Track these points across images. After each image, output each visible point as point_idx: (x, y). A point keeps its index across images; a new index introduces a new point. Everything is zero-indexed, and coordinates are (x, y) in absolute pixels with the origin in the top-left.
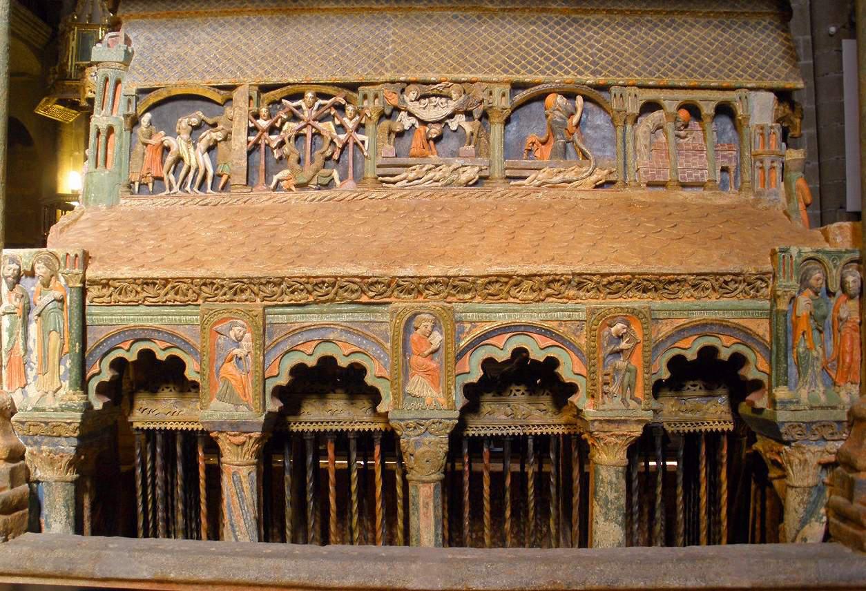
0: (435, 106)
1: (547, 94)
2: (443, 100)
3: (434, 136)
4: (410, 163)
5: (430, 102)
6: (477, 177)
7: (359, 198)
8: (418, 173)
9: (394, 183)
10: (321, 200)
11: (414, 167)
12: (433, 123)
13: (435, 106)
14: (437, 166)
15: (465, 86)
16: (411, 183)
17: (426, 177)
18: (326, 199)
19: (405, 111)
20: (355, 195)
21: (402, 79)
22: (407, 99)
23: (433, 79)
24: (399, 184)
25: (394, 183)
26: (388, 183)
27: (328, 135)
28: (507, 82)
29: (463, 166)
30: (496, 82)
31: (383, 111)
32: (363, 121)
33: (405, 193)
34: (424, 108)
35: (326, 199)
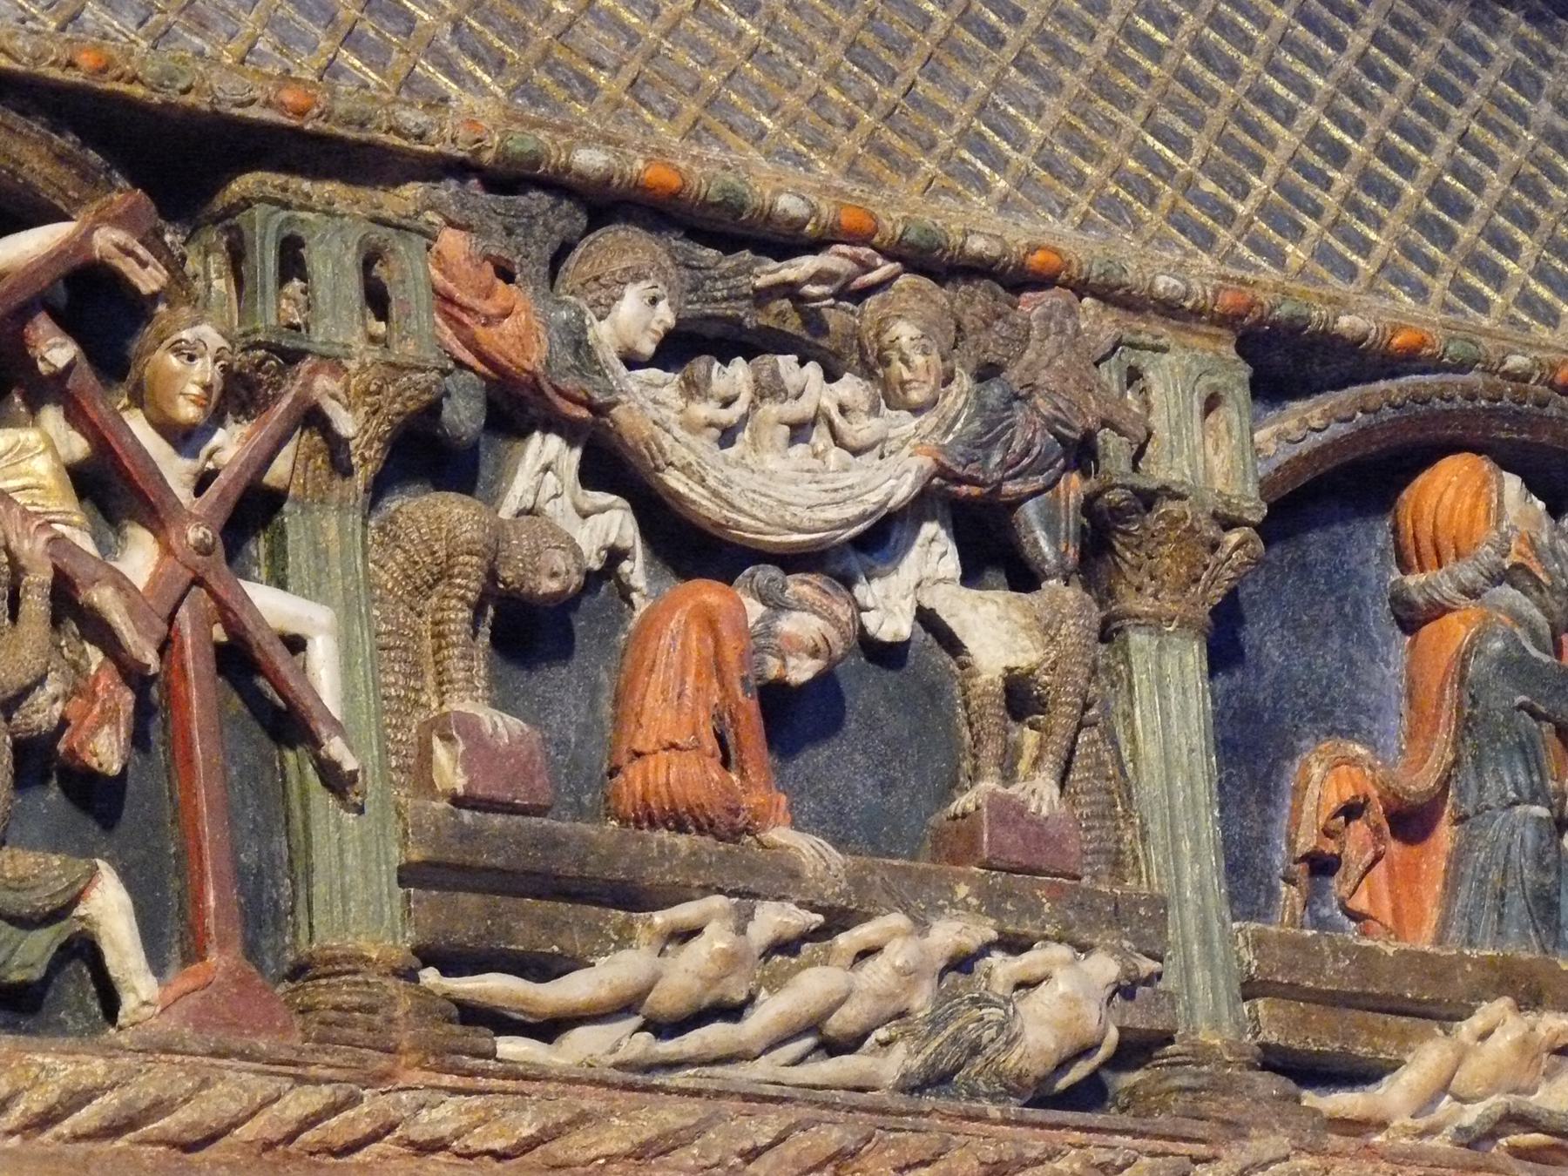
0: (799, 431)
1: (1425, 455)
2: (850, 387)
3: (802, 671)
4: (654, 875)
5: (770, 389)
6: (1113, 1034)
7: (336, 1128)
8: (732, 960)
9: (550, 1028)
10: (46, 1120)
11: (684, 913)
12: (794, 561)
13: (799, 431)
14: (837, 920)
15: (976, 299)
16: (690, 1043)
17: (769, 1012)
18: (86, 1117)
19: (570, 431)
20: (312, 1099)
21: (590, 159)
22: (604, 335)
23: (789, 204)
24: (583, 1044)
25: (550, 1028)
26: (500, 1021)
27: (32, 548)
28: (1226, 320)
29: (1014, 945)
30: (1169, 309)
31: (433, 410)
32: (280, 471)
33: (671, 1115)
34: (727, 436)
35: (86, 1117)
